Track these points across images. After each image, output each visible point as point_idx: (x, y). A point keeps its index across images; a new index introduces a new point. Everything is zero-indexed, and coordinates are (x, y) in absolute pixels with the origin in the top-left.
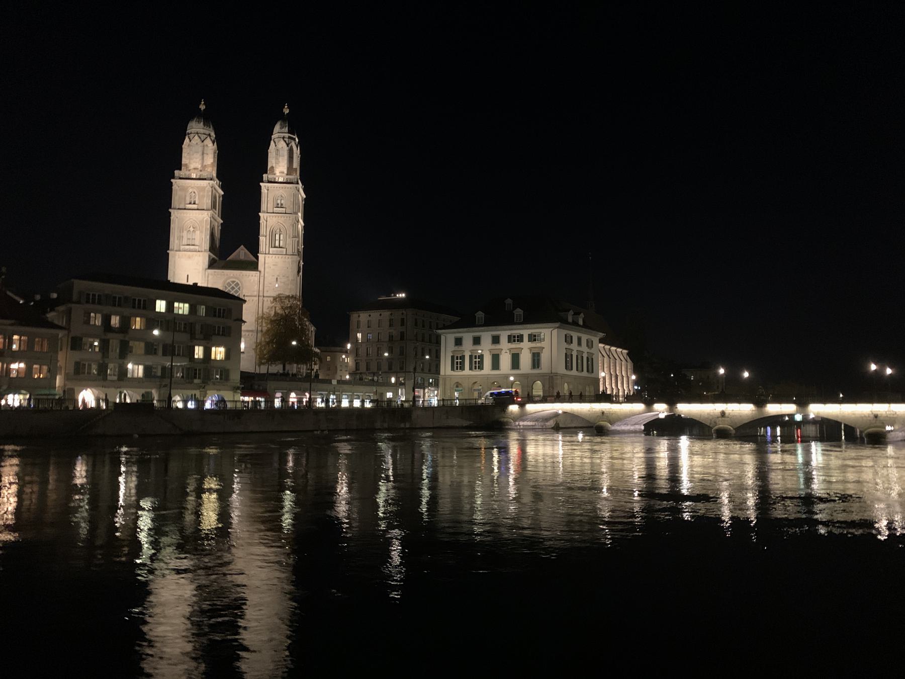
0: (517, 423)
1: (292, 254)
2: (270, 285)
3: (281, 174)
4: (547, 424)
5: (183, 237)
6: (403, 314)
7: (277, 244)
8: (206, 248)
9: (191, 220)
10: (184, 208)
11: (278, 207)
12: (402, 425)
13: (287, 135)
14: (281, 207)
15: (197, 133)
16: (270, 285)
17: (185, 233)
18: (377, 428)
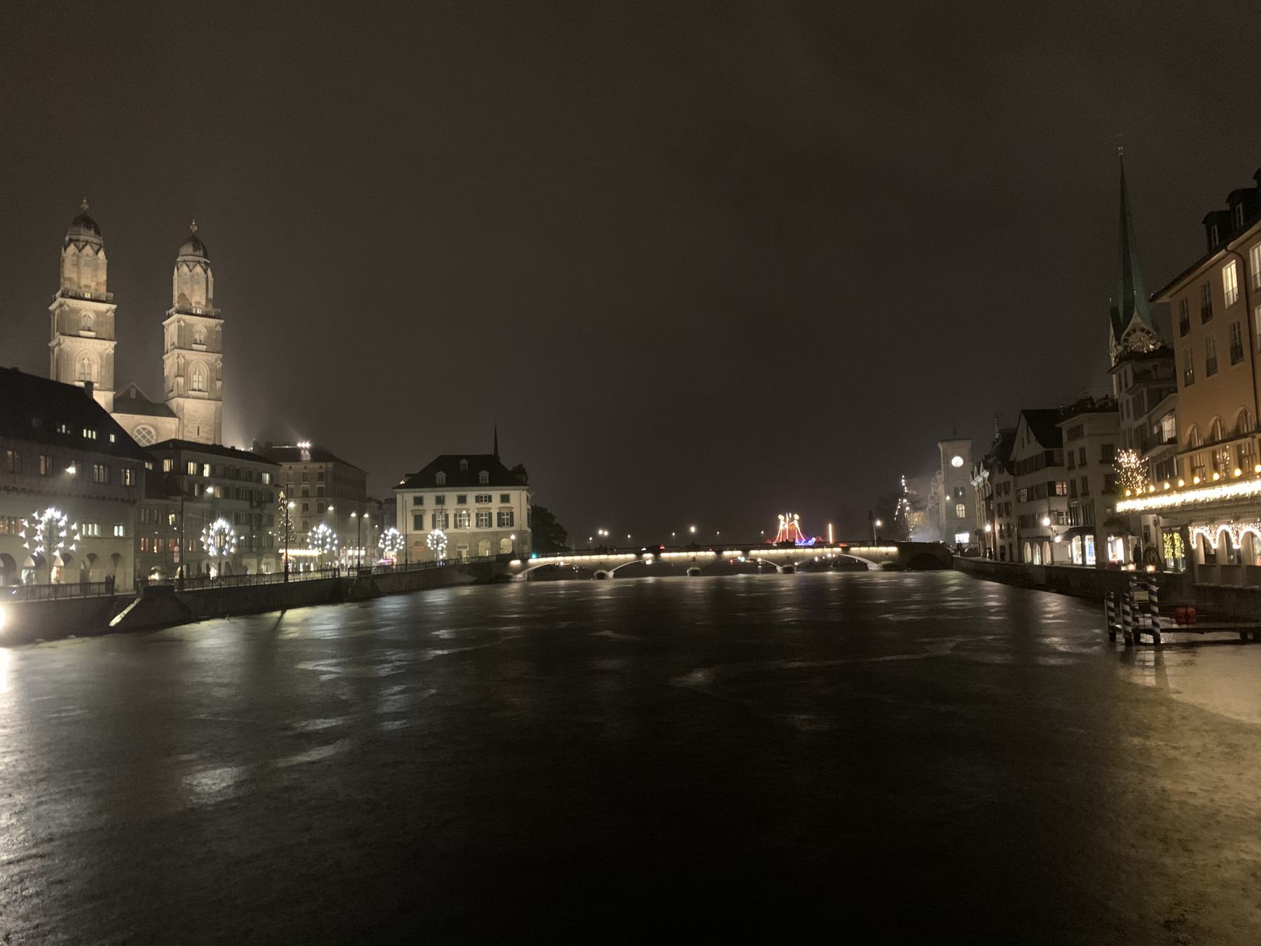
3: (197, 305)
6: (321, 467)
9: (86, 351)
10: (76, 334)
11: (197, 344)
13: (203, 260)
14: (200, 344)
15: (87, 242)
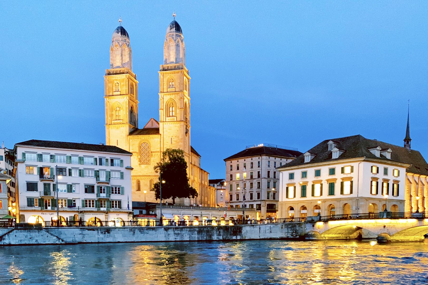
0: (323, 236)
1: (180, 120)
2: (167, 144)
4: (350, 235)
5: (113, 115)
7: (171, 115)
8: (127, 122)
12: (234, 238)
16: (167, 144)
17: (114, 113)
18: (214, 239)
